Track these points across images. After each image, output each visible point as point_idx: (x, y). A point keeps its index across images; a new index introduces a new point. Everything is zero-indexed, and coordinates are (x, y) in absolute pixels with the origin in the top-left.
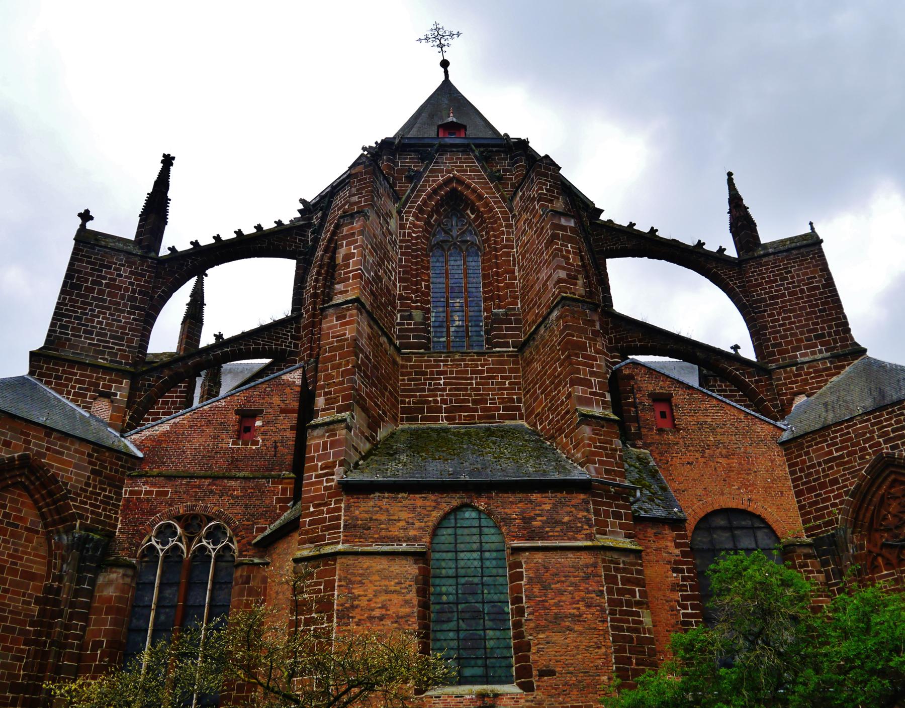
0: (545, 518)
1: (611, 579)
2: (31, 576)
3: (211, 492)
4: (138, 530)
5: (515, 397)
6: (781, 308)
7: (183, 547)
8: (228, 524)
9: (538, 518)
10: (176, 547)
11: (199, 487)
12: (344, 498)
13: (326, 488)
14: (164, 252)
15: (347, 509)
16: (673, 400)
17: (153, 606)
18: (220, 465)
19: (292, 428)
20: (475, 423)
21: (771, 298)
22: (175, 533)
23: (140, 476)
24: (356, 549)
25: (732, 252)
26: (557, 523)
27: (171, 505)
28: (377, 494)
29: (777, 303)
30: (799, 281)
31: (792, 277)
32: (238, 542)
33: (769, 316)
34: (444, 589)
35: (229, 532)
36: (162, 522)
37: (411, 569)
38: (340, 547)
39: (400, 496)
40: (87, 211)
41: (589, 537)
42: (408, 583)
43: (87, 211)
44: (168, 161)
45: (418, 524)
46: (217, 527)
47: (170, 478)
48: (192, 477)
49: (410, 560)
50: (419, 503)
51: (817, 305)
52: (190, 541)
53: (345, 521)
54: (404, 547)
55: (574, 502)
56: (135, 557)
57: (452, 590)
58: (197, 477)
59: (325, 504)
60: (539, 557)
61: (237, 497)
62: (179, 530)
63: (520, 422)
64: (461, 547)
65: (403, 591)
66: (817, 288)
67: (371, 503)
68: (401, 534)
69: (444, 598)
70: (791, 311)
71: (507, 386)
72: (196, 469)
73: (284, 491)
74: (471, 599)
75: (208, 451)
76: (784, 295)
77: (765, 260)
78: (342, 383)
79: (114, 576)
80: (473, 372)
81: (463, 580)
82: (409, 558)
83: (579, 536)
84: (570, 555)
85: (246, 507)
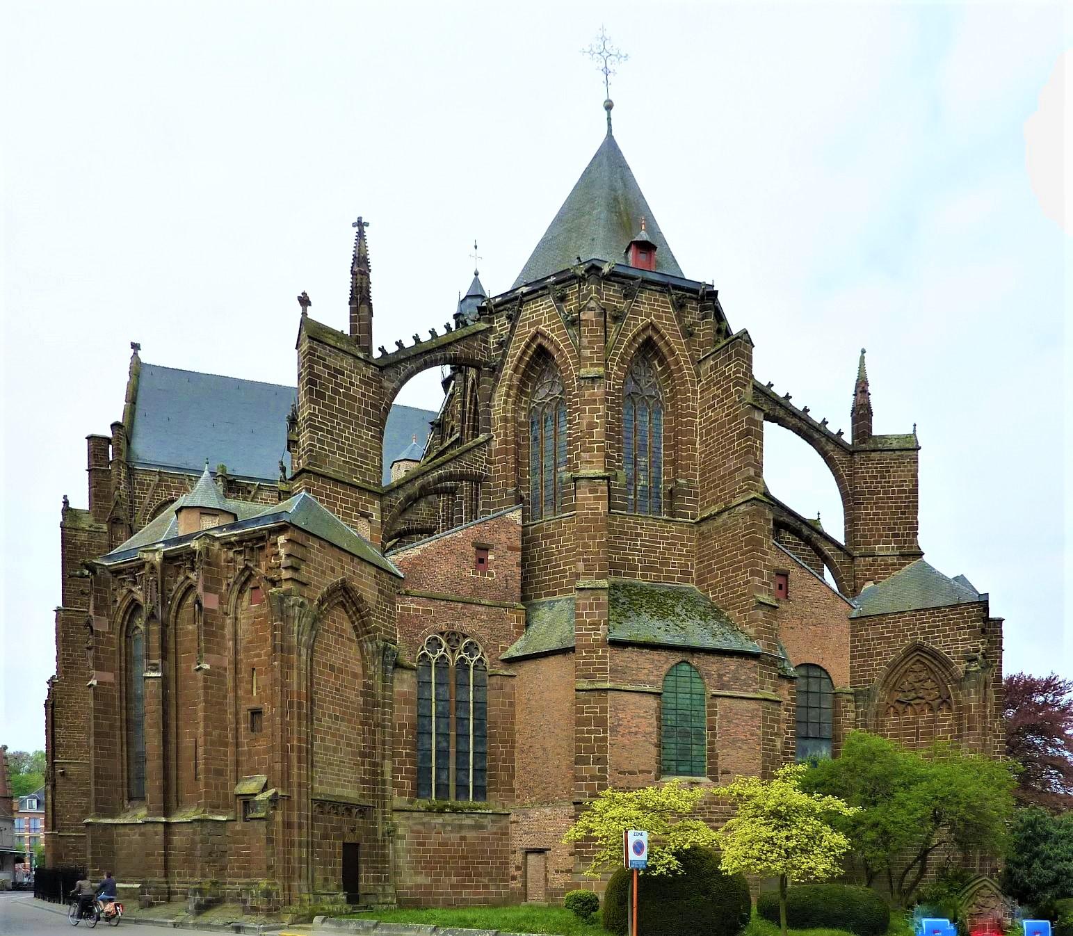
0: (731, 675)
1: (765, 719)
3: (464, 614)
4: (413, 641)
5: (689, 563)
6: (874, 503)
7: (449, 656)
8: (480, 642)
9: (727, 675)
10: (443, 657)
11: (454, 609)
13: (594, 640)
16: (790, 577)
17: (433, 700)
18: (466, 593)
20: (661, 582)
21: (870, 493)
22: (441, 646)
24: (619, 687)
26: (738, 679)
27: (434, 622)
28: (630, 648)
29: (872, 499)
30: (893, 482)
31: (890, 478)
32: (489, 657)
33: (866, 508)
34: (669, 717)
36: (430, 636)
37: (652, 703)
38: (608, 685)
39: (644, 651)
41: (755, 691)
42: (651, 712)
46: (471, 643)
47: (431, 598)
48: (447, 600)
49: (652, 696)
50: (656, 657)
51: (900, 508)
52: (453, 651)
53: (610, 666)
54: (648, 688)
55: (749, 666)
56: (415, 662)
57: (673, 717)
58: (452, 601)
59: (594, 652)
60: (727, 701)
61: (484, 621)
62: (444, 644)
63: (692, 585)
64: (679, 690)
65: (649, 717)
67: (626, 655)
69: (669, 722)
70: (881, 508)
71: (684, 553)
72: (447, 593)
74: (685, 724)
75: (455, 578)
76: (879, 492)
77: (873, 454)
79: (405, 676)
81: (679, 712)
82: (652, 696)
83: (750, 690)
84: (745, 702)
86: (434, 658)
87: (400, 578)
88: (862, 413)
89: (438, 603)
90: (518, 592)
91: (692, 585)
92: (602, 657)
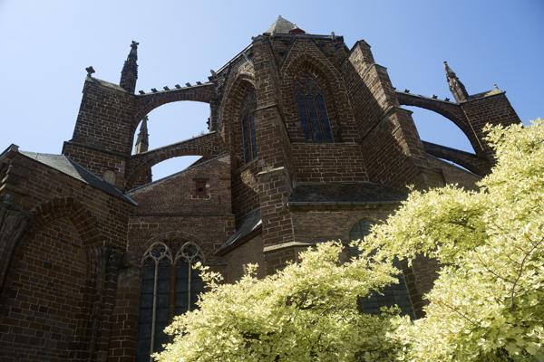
2: (76, 274)
3: (184, 224)
10: (165, 258)
12: (291, 214)
13: (277, 210)
14: (137, 93)
15: (295, 221)
19: (228, 188)
23: (139, 215)
25: (453, 100)
35: (199, 249)
40: (91, 68)
43: (91, 68)
44: (134, 46)
45: (339, 229)
46: (190, 246)
66: (506, 116)
68: (330, 234)
73: (229, 224)
78: (275, 151)
80: (336, 155)
85: (207, 233)
86: (157, 261)
87: (134, 205)
88: (458, 87)
89: (163, 219)
90: (229, 205)
91: (365, 182)
92: (286, 222)
